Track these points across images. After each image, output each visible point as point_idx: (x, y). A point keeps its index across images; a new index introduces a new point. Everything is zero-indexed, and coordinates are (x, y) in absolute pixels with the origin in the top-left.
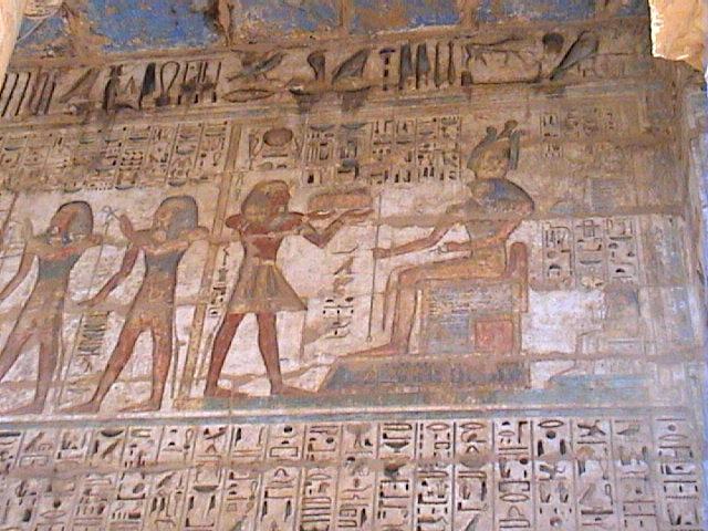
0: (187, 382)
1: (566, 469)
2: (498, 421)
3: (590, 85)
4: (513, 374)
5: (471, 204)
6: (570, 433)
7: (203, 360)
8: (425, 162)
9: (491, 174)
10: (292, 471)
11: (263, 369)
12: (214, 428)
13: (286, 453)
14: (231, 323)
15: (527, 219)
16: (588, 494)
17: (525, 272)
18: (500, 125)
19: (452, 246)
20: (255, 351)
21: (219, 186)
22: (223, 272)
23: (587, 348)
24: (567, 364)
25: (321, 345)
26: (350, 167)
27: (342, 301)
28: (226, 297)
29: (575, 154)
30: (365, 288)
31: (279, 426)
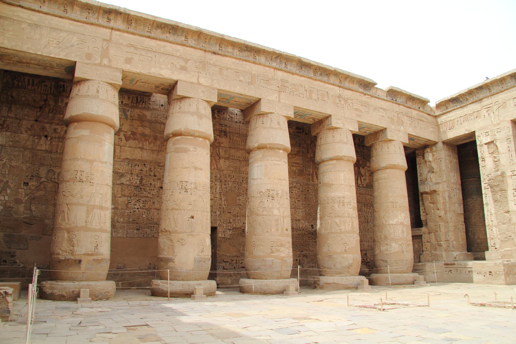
14: (358, 177)
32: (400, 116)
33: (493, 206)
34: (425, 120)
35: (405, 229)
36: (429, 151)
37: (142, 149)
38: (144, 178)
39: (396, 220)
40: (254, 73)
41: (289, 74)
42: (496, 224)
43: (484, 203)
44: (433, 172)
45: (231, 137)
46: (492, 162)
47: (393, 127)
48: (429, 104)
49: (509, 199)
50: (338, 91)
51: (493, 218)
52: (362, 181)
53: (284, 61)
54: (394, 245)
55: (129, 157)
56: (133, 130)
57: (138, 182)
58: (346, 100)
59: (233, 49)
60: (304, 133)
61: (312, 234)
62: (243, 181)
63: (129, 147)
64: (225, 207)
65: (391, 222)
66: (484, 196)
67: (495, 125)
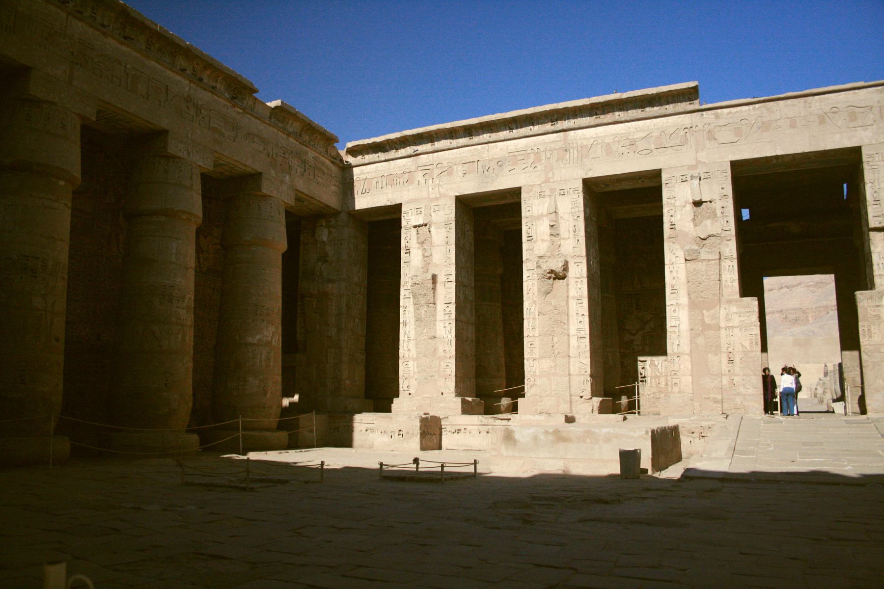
32: (287, 156)
33: (413, 327)
34: (326, 171)
36: (324, 224)
39: (258, 337)
42: (415, 356)
43: (401, 321)
44: (326, 261)
46: (420, 258)
47: (273, 172)
48: (335, 145)
49: (438, 318)
50: (187, 89)
51: (412, 345)
54: (251, 379)
65: (250, 340)
66: (402, 310)
67: (431, 200)
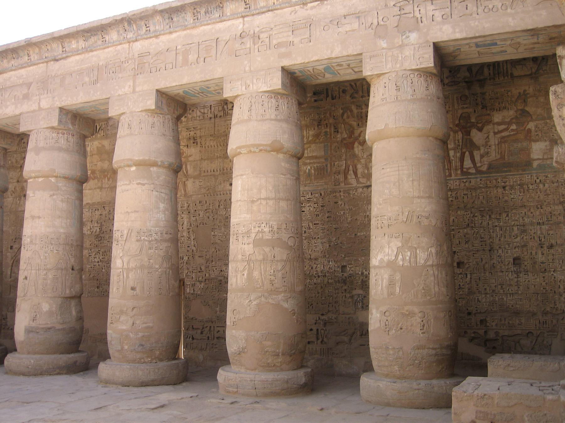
0: (456, 170)
1: (541, 186)
2: (526, 176)
3: (546, 76)
4: (529, 163)
5: (516, 118)
6: (542, 178)
7: (459, 164)
8: (503, 105)
9: (521, 108)
10: (483, 190)
11: (472, 166)
12: (465, 181)
13: (481, 185)
14: (463, 155)
15: (530, 121)
16: (546, 191)
17: (530, 137)
18: (522, 92)
19: (513, 130)
20: (470, 161)
21: (452, 114)
22: (458, 140)
23: (545, 157)
24: (541, 161)
25: (485, 159)
26: (484, 107)
27: (488, 147)
28: (460, 147)
29: (542, 100)
30: (493, 143)
31: (478, 180)
35: (398, 277)
37: (101, 188)
38: (103, 223)
40: (101, 64)
41: (151, 40)
45: (203, 143)
47: (383, 44)
50: (241, 26)
52: (477, 158)
53: (143, 23)
55: (89, 202)
56: (93, 168)
57: (98, 230)
58: (256, 37)
59: (78, 42)
60: (329, 99)
61: (344, 282)
62: (219, 206)
63: (89, 189)
64: (194, 249)
